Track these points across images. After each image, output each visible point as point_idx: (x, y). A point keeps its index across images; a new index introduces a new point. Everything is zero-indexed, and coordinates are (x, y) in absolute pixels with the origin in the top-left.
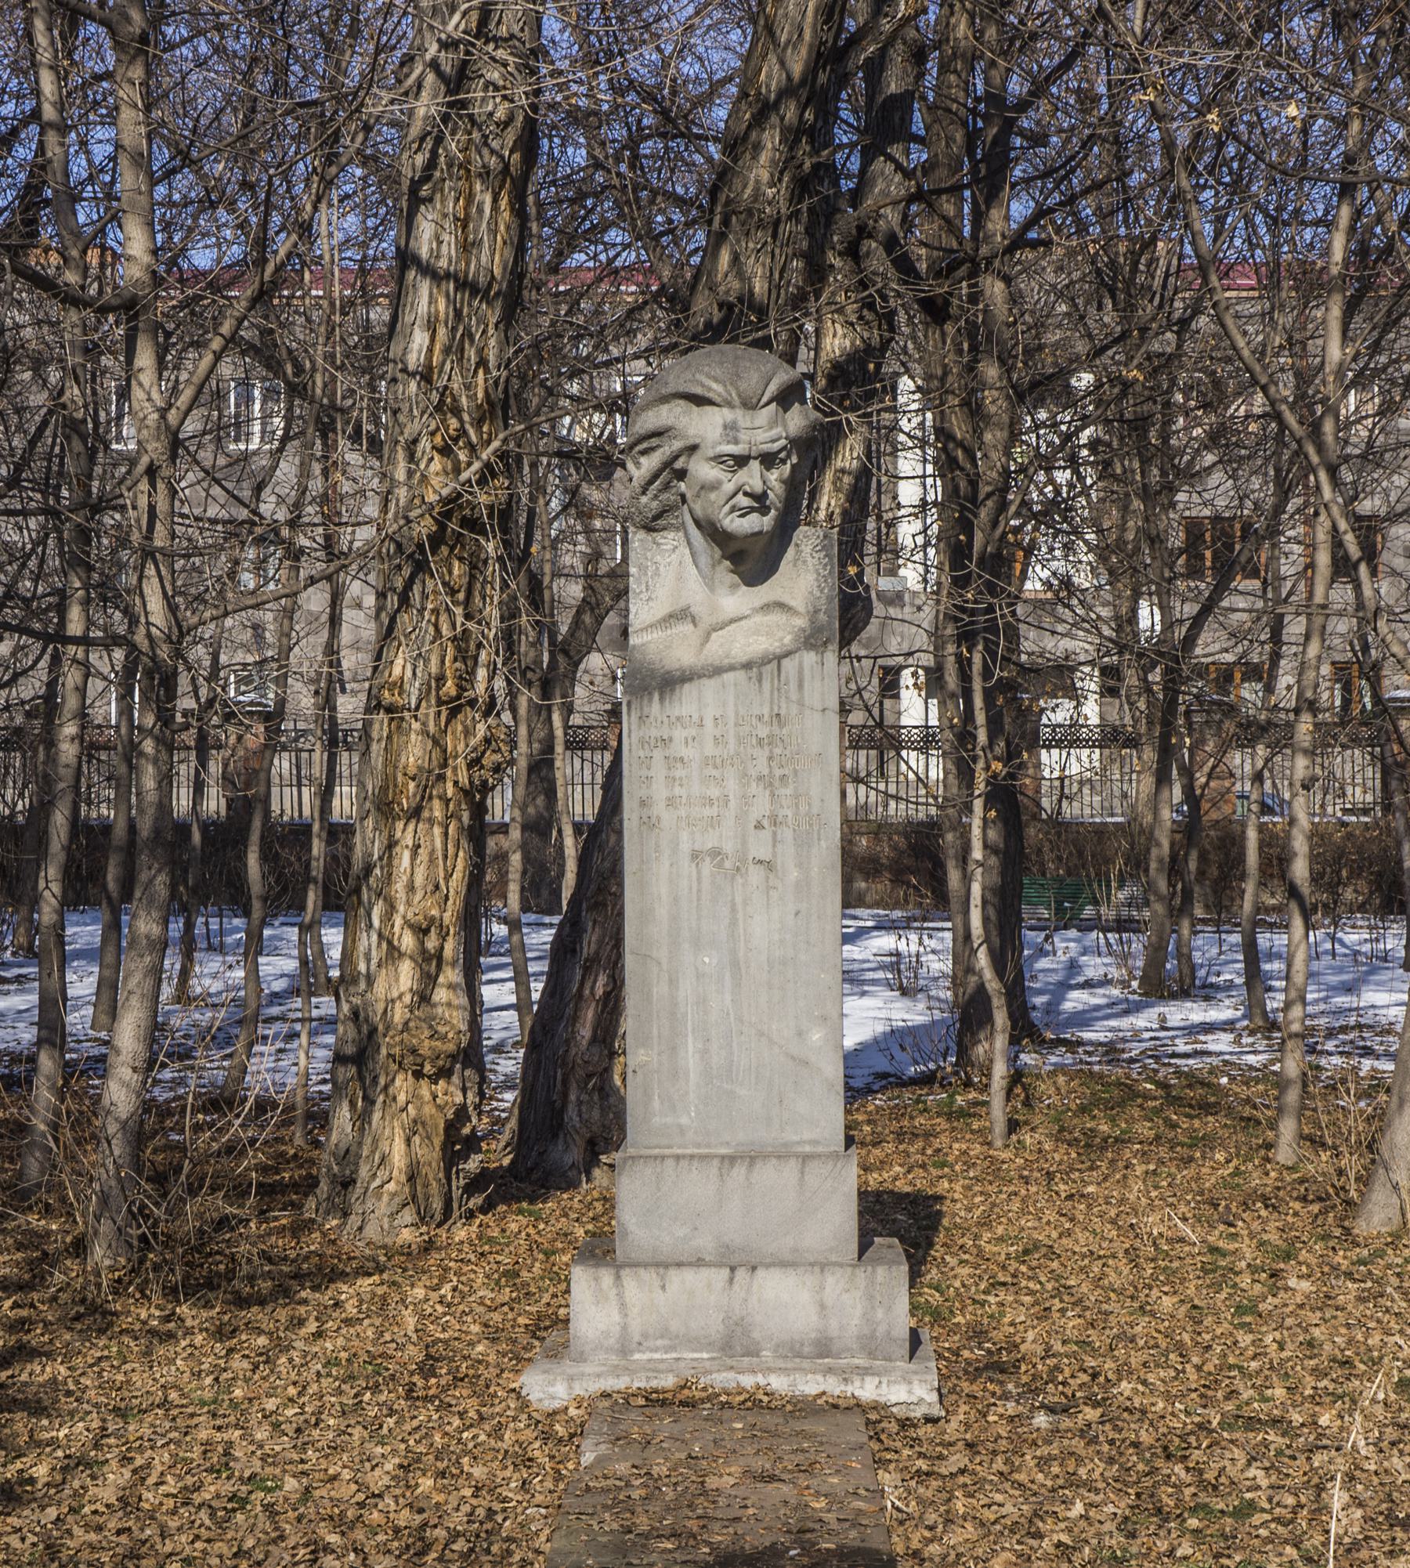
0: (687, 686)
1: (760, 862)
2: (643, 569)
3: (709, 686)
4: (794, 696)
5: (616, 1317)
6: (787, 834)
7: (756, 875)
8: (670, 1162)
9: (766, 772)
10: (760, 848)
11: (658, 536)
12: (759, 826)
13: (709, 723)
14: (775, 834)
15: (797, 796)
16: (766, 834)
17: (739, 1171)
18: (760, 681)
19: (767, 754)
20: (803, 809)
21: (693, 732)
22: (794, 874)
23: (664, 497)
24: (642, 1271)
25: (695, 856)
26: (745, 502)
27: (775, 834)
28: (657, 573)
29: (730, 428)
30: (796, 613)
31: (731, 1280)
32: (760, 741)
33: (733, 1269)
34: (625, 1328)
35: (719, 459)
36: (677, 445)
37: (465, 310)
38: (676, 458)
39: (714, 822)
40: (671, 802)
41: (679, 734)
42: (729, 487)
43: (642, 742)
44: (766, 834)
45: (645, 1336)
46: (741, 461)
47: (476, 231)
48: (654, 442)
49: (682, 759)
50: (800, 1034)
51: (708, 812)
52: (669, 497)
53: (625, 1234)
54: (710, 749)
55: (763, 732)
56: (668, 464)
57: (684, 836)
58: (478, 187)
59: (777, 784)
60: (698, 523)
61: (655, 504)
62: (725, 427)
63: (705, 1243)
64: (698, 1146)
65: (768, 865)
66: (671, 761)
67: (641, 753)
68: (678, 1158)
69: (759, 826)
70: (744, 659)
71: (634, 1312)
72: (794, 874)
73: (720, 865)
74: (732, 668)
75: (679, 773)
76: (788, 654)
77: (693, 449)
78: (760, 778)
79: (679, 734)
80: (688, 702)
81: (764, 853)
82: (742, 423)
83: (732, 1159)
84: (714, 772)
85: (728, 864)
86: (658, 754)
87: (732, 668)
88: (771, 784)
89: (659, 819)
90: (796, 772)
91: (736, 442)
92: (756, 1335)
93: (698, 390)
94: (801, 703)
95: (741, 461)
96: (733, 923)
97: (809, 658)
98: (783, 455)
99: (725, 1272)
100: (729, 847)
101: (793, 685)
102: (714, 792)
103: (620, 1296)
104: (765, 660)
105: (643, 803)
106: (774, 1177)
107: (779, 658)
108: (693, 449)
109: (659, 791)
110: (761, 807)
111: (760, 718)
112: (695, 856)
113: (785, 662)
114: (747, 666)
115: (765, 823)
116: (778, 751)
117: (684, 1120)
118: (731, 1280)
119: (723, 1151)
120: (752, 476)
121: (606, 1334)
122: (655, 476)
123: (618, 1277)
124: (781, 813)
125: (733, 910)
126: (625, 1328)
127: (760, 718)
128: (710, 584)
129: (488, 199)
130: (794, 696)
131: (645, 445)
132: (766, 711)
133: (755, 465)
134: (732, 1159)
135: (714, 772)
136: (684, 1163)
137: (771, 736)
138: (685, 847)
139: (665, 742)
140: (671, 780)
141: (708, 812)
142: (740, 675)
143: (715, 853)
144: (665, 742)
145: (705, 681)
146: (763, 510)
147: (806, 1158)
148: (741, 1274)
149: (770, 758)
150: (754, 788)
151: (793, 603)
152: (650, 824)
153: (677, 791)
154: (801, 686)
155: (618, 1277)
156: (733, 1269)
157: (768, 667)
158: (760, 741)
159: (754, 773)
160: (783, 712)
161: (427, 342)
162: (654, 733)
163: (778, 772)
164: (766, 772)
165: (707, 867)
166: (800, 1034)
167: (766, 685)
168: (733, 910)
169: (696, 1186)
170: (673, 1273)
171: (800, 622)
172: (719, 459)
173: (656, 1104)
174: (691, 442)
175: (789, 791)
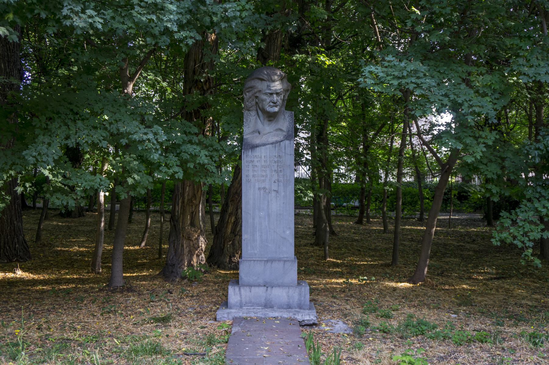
3: (263, 148)
4: (283, 151)
5: (239, 299)
6: (281, 184)
7: (274, 194)
8: (252, 262)
10: (274, 187)
12: (275, 182)
13: (263, 157)
15: (284, 175)
16: (276, 184)
17: (269, 264)
20: (285, 178)
22: (283, 194)
24: (245, 288)
25: (259, 189)
26: (272, 104)
30: (284, 131)
31: (267, 290)
33: (267, 287)
34: (241, 301)
36: (256, 90)
39: (264, 181)
40: (254, 176)
41: (256, 160)
43: (247, 162)
44: (276, 184)
45: (246, 303)
46: (271, 94)
48: (250, 89)
50: (284, 232)
51: (262, 178)
53: (242, 279)
54: (263, 163)
57: (257, 184)
60: (260, 109)
63: (261, 281)
64: (259, 258)
65: (277, 192)
66: (254, 166)
68: (254, 261)
69: (275, 182)
71: (243, 297)
72: (283, 194)
73: (265, 191)
74: (268, 144)
75: (256, 169)
76: (282, 141)
77: (260, 91)
78: (275, 171)
79: (256, 160)
80: (259, 152)
81: (276, 189)
83: (267, 261)
85: (267, 191)
86: (250, 164)
92: (273, 303)
93: (261, 77)
94: (285, 153)
96: (268, 205)
97: (287, 142)
99: (266, 288)
100: (267, 187)
101: (283, 148)
102: (264, 174)
103: (240, 293)
104: (277, 142)
105: (247, 176)
106: (278, 266)
109: (251, 173)
110: (275, 177)
111: (275, 156)
112: (259, 189)
113: (281, 143)
114: (272, 144)
117: (256, 252)
118: (267, 290)
119: (265, 259)
120: (275, 97)
121: (237, 302)
123: (240, 289)
124: (280, 179)
125: (268, 202)
126: (241, 301)
127: (275, 156)
130: (283, 151)
132: (277, 155)
133: (275, 96)
134: (267, 261)
136: (256, 262)
138: (257, 187)
139: (252, 161)
140: (254, 171)
141: (262, 178)
142: (270, 146)
143: (264, 188)
144: (252, 161)
146: (276, 106)
147: (285, 261)
148: (269, 289)
150: (274, 173)
152: (249, 181)
153: (255, 173)
154: (285, 149)
155: (240, 289)
156: (267, 287)
158: (275, 162)
159: (273, 169)
162: (250, 159)
163: (279, 169)
165: (262, 192)
166: (284, 232)
167: (277, 148)
168: (268, 202)
169: (259, 268)
170: (253, 288)
173: (249, 248)
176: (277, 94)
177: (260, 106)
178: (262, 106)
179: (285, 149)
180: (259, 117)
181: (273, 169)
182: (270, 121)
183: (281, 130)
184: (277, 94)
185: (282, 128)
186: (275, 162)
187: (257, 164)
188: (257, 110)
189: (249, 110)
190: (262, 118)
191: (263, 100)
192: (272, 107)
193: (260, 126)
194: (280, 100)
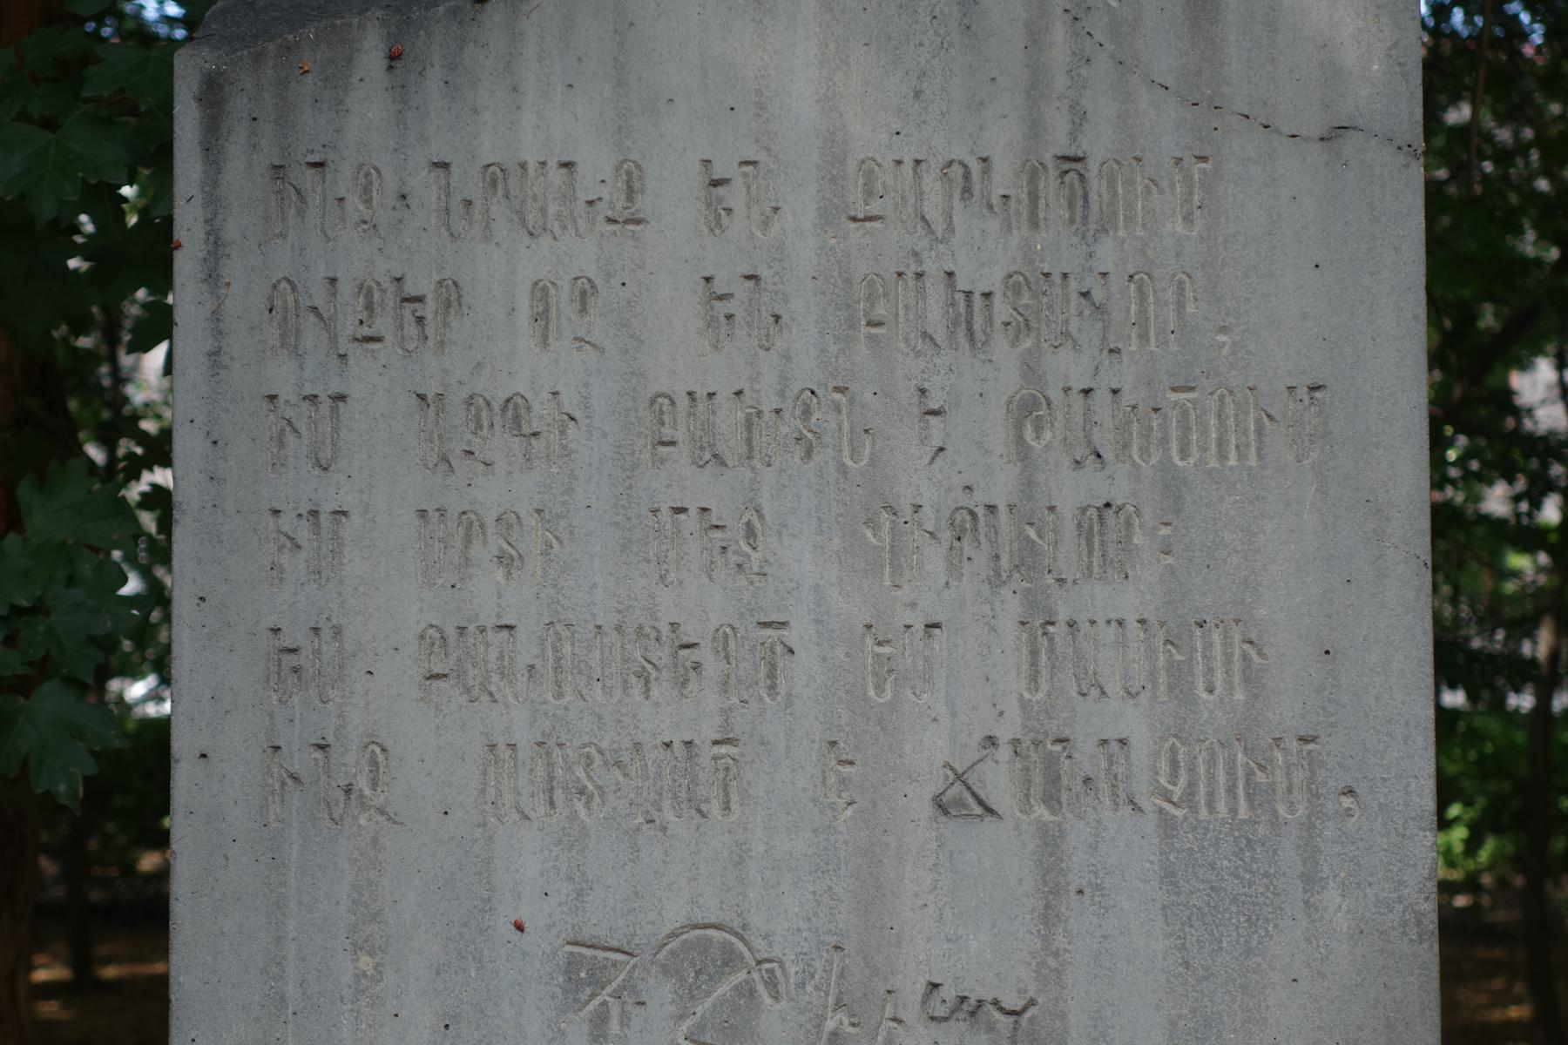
1: (971, 1010)
9: (1001, 487)
12: (960, 801)
13: (673, 199)
14: (1051, 841)
16: (1001, 851)
19: (1008, 380)
21: (582, 254)
25: (588, 970)
27: (1051, 841)
32: (968, 316)
40: (449, 659)
41: (504, 268)
44: (1001, 851)
49: (514, 411)
51: (664, 715)
55: (984, 254)
59: (1068, 555)
67: (283, 377)
69: (960, 801)
75: (508, 486)
78: (966, 524)
84: (699, 488)
88: (1028, 560)
89: (377, 755)
90: (1173, 487)
102: (700, 602)
105: (287, 662)
111: (965, 181)
115: (998, 782)
116: (1068, 367)
127: (965, 181)
132: (1002, 140)
135: (699, 488)
137: (1028, 282)
141: (664, 715)
149: (1028, 410)
153: (488, 592)
159: (922, 485)
160: (1098, 145)
163: (1071, 491)
164: (1001, 487)
175: (1129, 601)
181: (922, 485)
186: (968, 316)
187: (529, 368)
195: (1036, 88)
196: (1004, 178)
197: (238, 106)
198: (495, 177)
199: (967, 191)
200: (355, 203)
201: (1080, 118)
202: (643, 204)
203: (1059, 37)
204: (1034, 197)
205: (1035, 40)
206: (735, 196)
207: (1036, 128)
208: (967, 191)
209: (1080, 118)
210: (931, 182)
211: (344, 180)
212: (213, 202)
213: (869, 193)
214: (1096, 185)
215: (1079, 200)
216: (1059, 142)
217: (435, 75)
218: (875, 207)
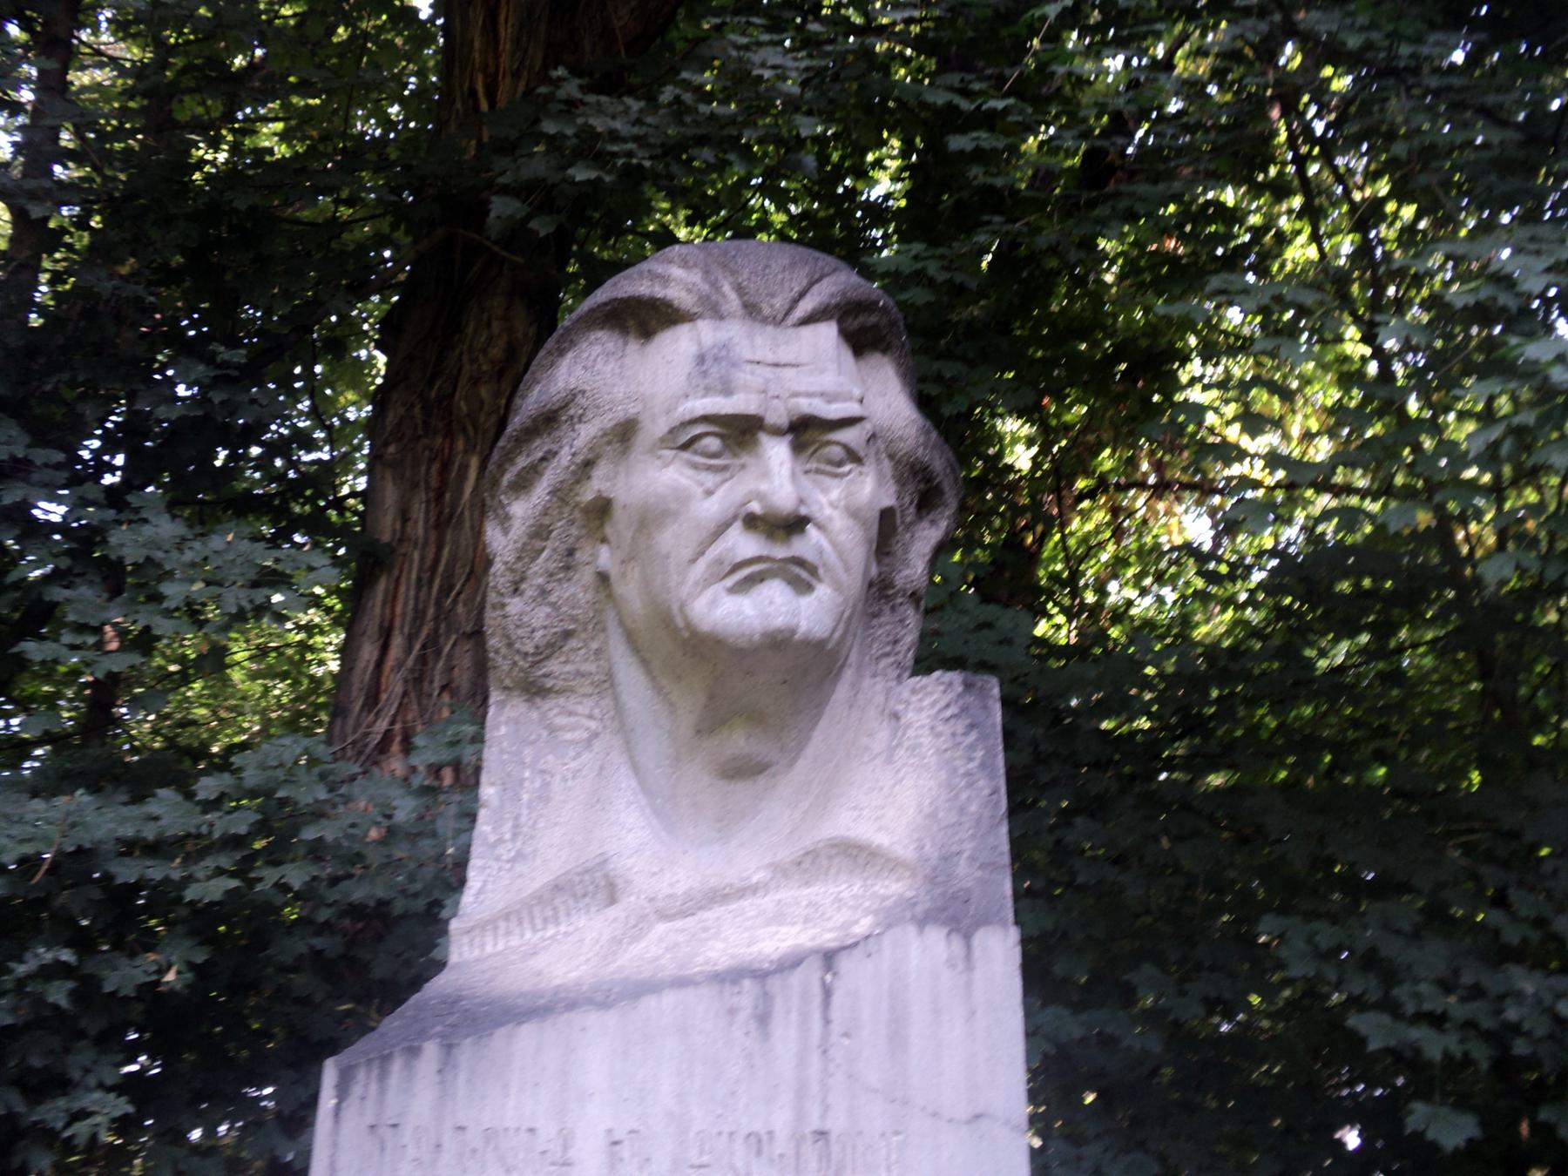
0: (527, 1031)
2: (511, 787)
11: (551, 708)
18: (763, 1019)
23: (560, 593)
26: (743, 544)
28: (543, 796)
29: (712, 368)
35: (683, 439)
36: (586, 433)
37: (431, 611)
38: (588, 464)
42: (711, 508)
46: (741, 432)
47: (454, 507)
48: (539, 448)
52: (577, 591)
56: (561, 494)
58: (460, 445)
61: (540, 616)
62: (701, 359)
70: (724, 963)
74: (681, 983)
77: (625, 433)
82: (744, 349)
87: (681, 983)
91: (727, 391)
95: (741, 432)
97: (928, 950)
98: (848, 436)
107: (829, 958)
108: (625, 433)
111: (758, 1143)
113: (845, 964)
114: (731, 977)
120: (776, 473)
122: (540, 532)
128: (733, 957)
129: (474, 462)
131: (522, 462)
132: (781, 1120)
133: (777, 452)
142: (701, 1002)
145: (592, 1018)
146: (801, 575)
151: (882, 840)
154: (897, 1039)
157: (796, 978)
160: (837, 1123)
161: (374, 658)
167: (785, 1034)
171: (894, 887)
172: (683, 439)
174: (620, 414)
176: (806, 432)
177: (629, 589)
178: (646, 583)
179: (897, 1039)
180: (629, 749)
182: (741, 770)
183: (856, 855)
184: (806, 432)
185: (864, 830)
188: (607, 683)
189: (534, 690)
190: (653, 746)
191: (651, 519)
192: (749, 577)
193: (630, 835)
194: (839, 522)
195: (801, 1093)
196: (782, 1145)
197: (356, 1090)
198: (490, 1135)
199: (759, 1152)
200: (412, 1152)
201: (826, 1109)
202: (572, 1153)
203: (815, 1059)
204: (798, 1155)
205: (801, 1063)
206: (624, 1151)
207: (800, 1115)
208: (759, 1152)
209: (826, 1109)
210: (739, 1146)
211: (407, 1135)
212: (335, 1145)
213: (702, 1152)
214: (835, 1149)
215: (825, 1157)
216: (814, 1123)
217: (462, 1077)
218: (705, 1159)
